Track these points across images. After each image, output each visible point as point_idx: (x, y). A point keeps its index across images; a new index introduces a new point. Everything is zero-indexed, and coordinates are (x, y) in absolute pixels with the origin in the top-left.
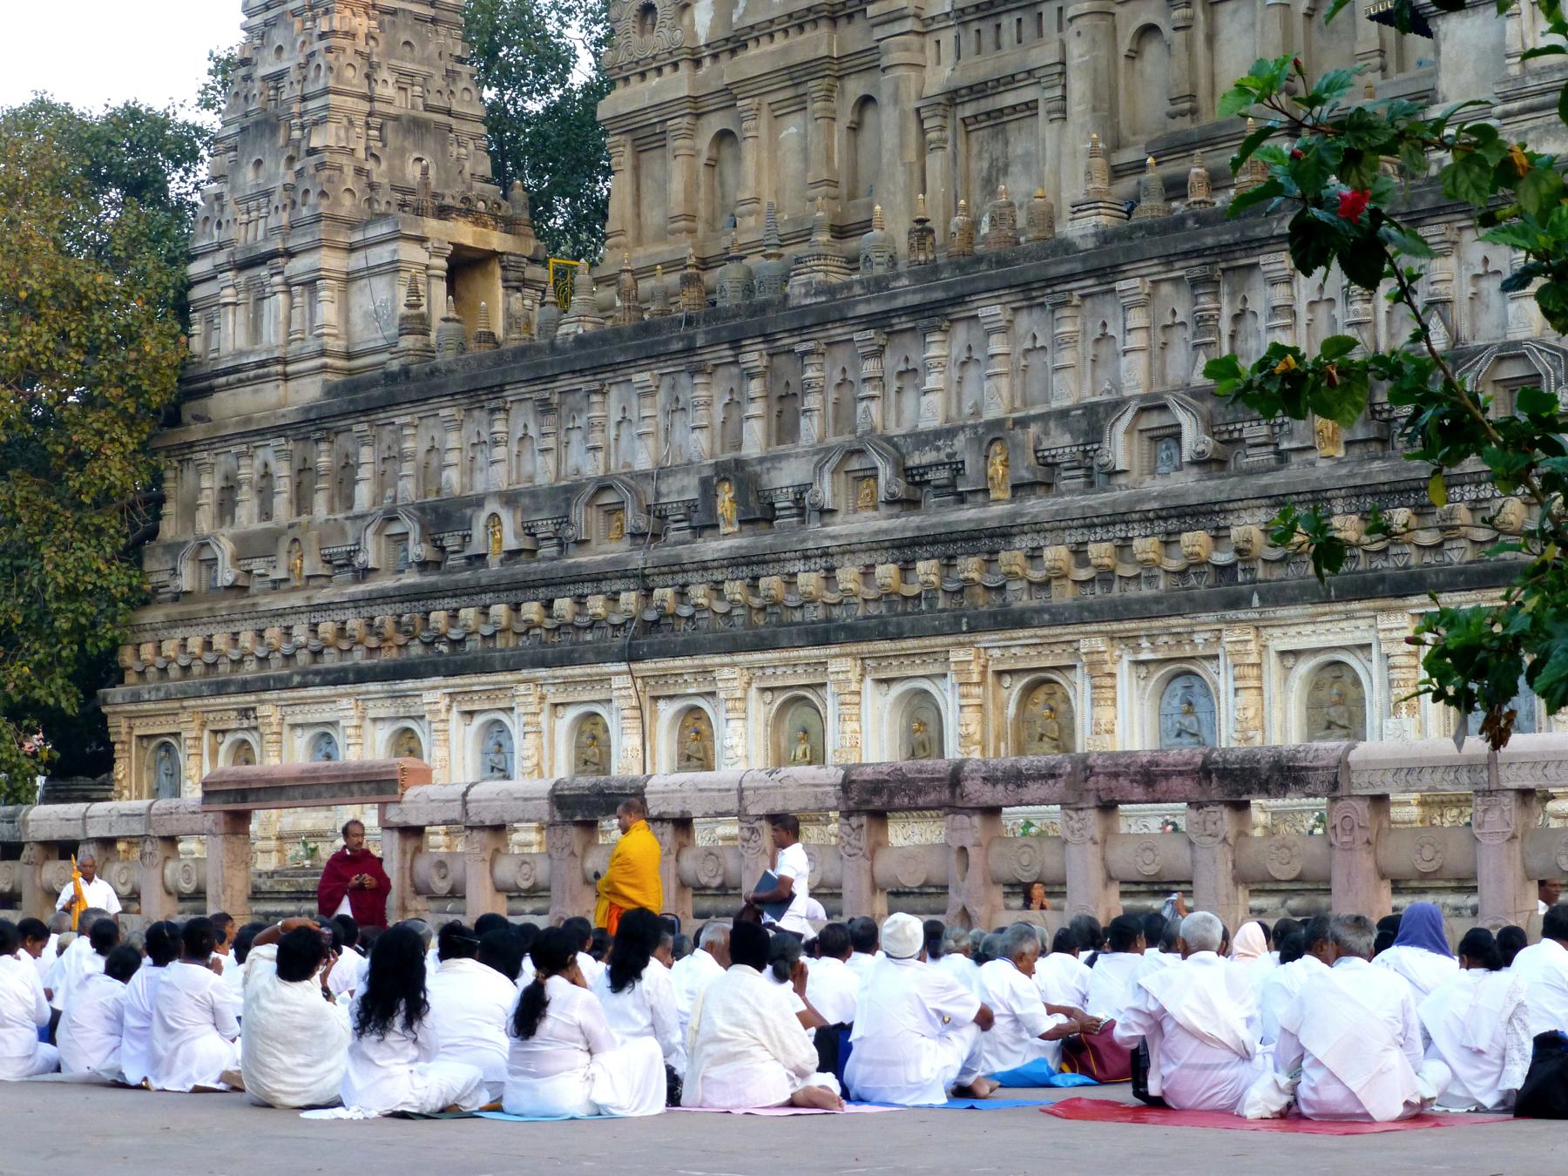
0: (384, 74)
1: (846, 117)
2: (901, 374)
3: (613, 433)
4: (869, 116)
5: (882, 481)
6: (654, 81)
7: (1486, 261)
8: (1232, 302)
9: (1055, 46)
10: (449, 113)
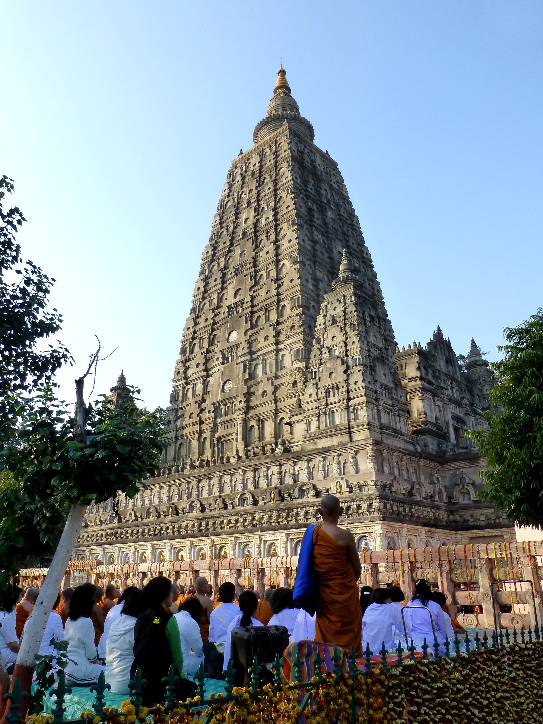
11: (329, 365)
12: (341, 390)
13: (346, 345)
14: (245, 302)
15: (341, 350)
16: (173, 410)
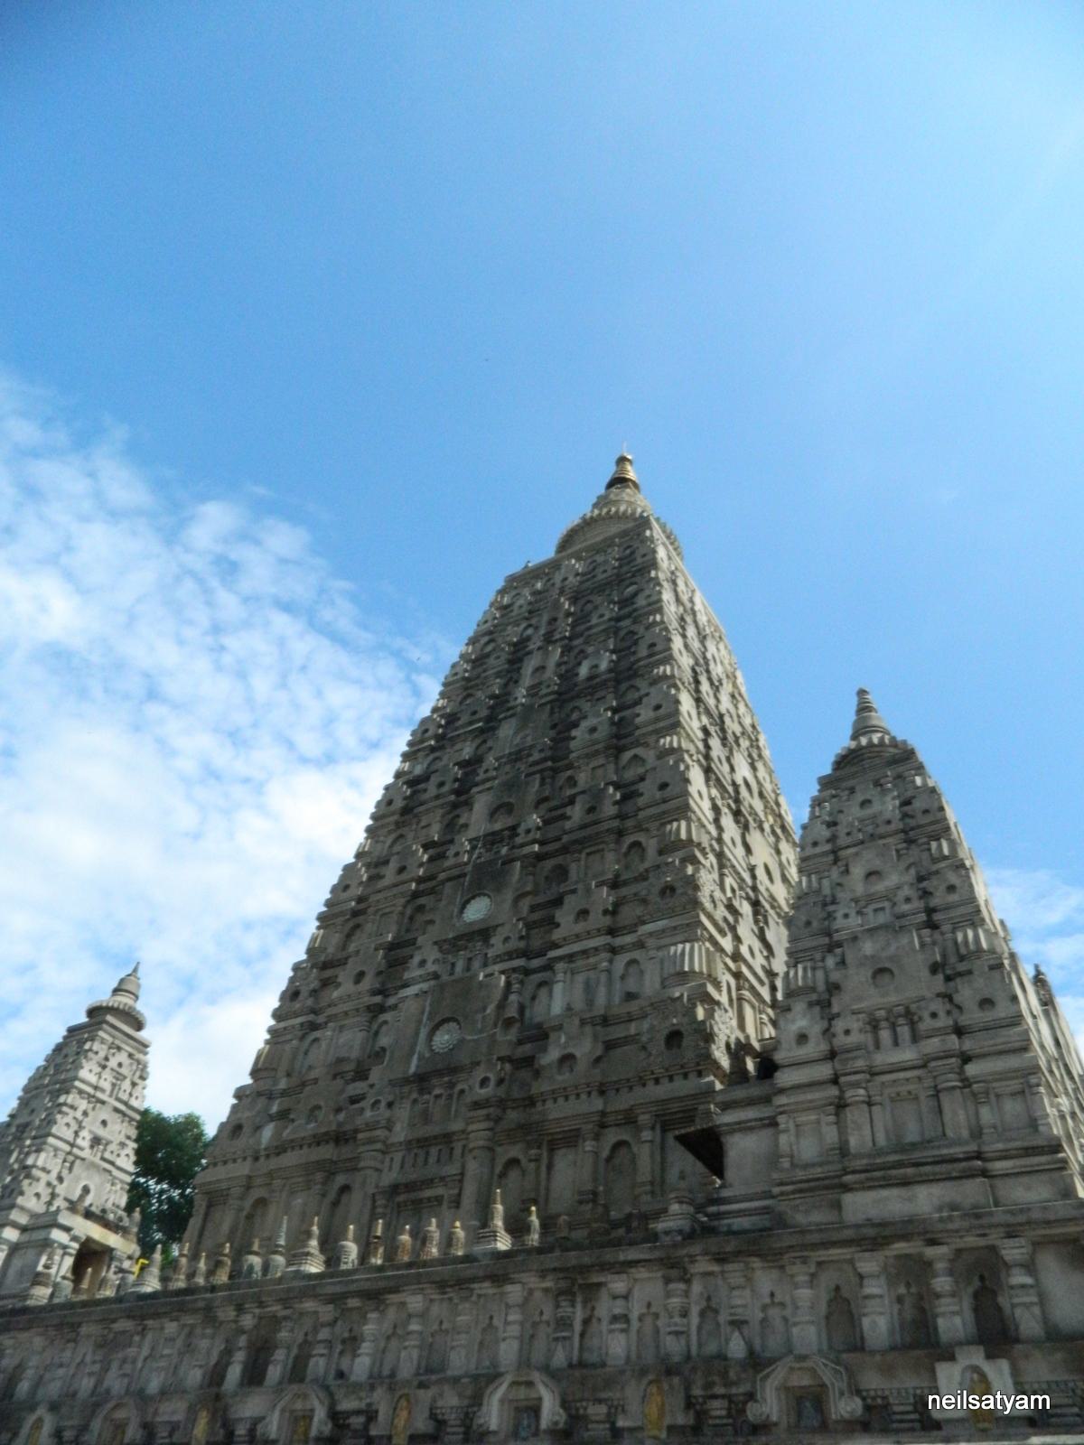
0: (84, 1133)
1: (332, 1196)
2: (344, 1342)
3: (139, 1365)
4: (345, 1198)
5: (316, 1419)
6: (230, 1166)
7: (772, 1295)
8: (584, 1307)
9: (458, 1165)
10: (112, 1163)
11: (868, 947)
12: (926, 1024)
13: (926, 894)
14: (521, 830)
15: (906, 907)
16: (259, 1094)
